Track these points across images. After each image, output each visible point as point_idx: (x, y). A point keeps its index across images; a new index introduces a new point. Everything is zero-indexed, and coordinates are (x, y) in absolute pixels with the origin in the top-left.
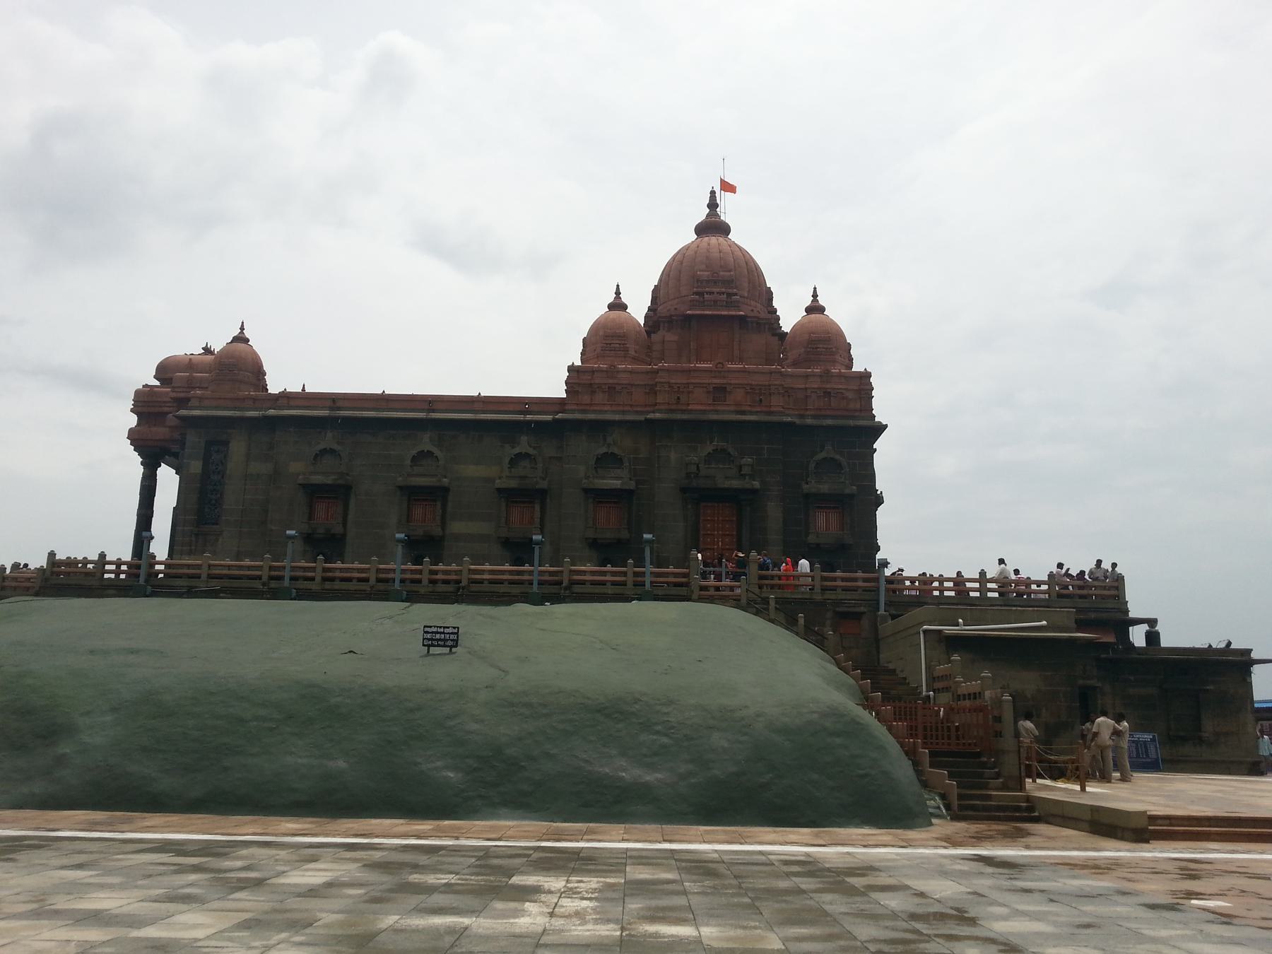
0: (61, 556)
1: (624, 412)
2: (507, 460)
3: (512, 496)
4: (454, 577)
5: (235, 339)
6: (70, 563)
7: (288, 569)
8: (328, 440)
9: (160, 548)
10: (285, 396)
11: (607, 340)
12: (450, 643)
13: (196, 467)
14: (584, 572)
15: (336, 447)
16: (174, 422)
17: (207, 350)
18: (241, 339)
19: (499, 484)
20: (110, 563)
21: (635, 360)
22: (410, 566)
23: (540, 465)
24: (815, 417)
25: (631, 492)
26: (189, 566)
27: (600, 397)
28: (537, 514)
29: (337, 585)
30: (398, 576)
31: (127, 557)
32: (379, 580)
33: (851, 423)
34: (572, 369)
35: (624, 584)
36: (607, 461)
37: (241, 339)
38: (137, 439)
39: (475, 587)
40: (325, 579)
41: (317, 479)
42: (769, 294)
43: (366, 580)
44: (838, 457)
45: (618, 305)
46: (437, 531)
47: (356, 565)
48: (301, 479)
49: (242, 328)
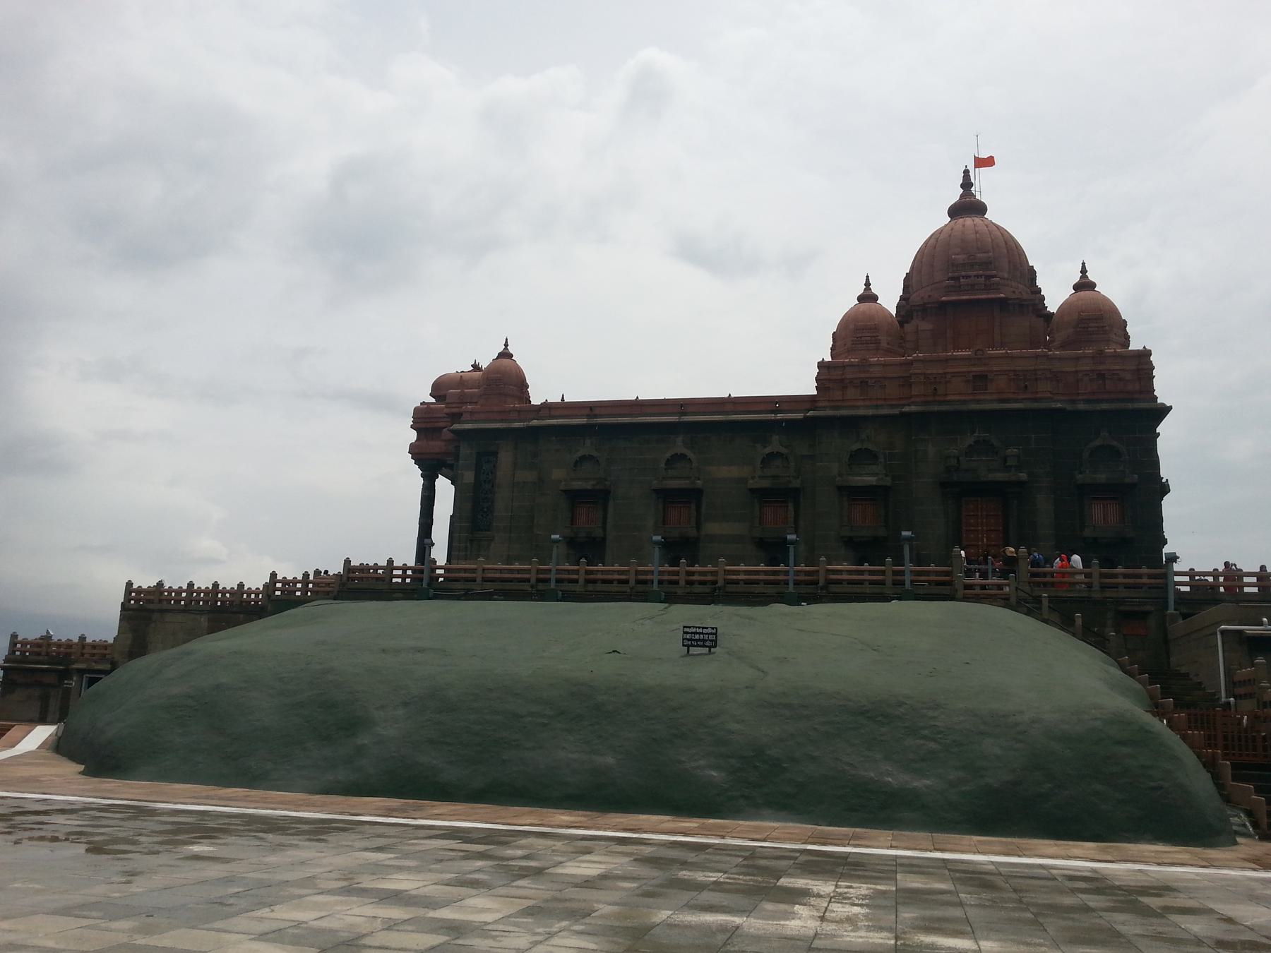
0: (355, 563)
1: (877, 407)
3: (763, 496)
4: (709, 578)
5: (501, 355)
6: (363, 568)
7: (554, 572)
8: (587, 447)
9: (440, 554)
10: (547, 407)
11: (859, 333)
12: (708, 643)
13: (469, 477)
14: (840, 572)
15: (594, 453)
16: (451, 436)
17: (476, 367)
18: (505, 355)
19: (752, 484)
20: (398, 568)
21: (888, 352)
22: (667, 568)
24: (1088, 401)
25: (886, 489)
26: (465, 570)
27: (851, 393)
28: (791, 514)
29: (600, 587)
30: (656, 578)
31: (411, 562)
32: (638, 582)
33: (1130, 406)
34: (821, 365)
35: (882, 583)
36: (860, 458)
37: (505, 355)
38: (417, 453)
39: (731, 588)
40: (588, 581)
41: (577, 485)
42: (1032, 273)
43: (626, 582)
44: (1114, 443)
45: (868, 297)
46: (692, 533)
47: (617, 567)
49: (506, 345)
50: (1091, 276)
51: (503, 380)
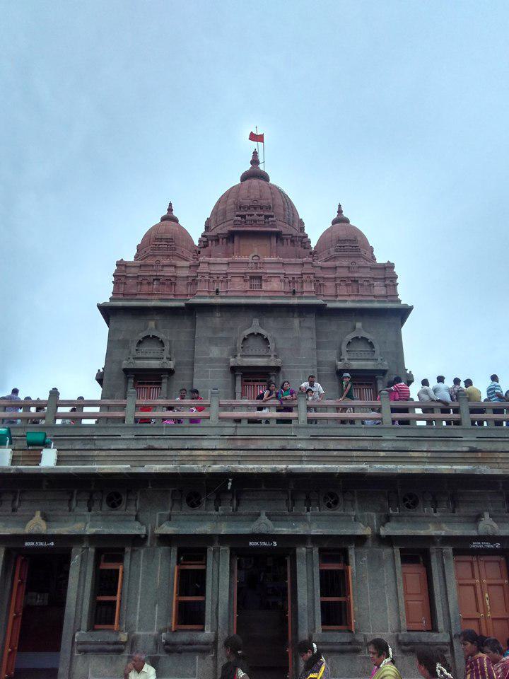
25: (170, 372)
34: (121, 264)
50: (345, 214)
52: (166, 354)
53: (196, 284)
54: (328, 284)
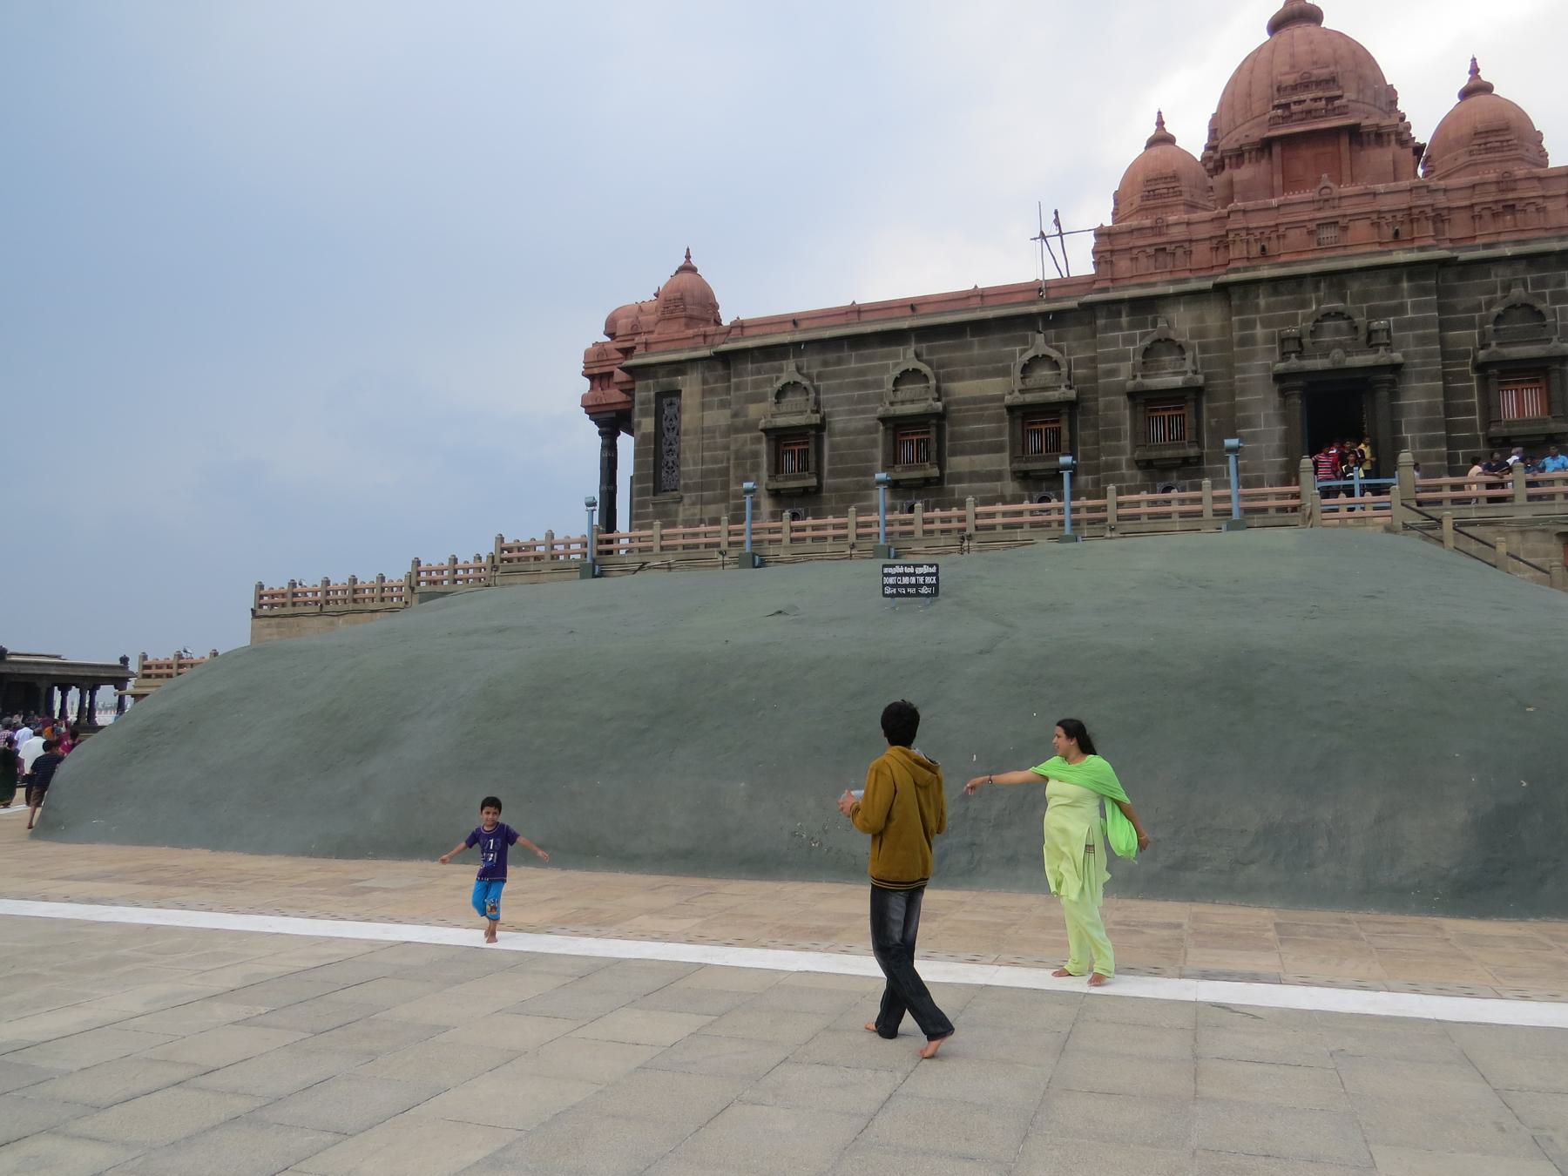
0: (509, 541)
2: (1019, 368)
4: (955, 524)
5: (682, 269)
8: (788, 371)
10: (740, 326)
12: (924, 590)
18: (687, 268)
19: (1008, 399)
23: (1064, 370)
25: (1199, 391)
34: (1101, 233)
37: (687, 268)
41: (781, 421)
45: (1162, 139)
48: (762, 424)
49: (688, 257)
50: (1485, 76)
51: (688, 302)
52: (1188, 365)
53: (1227, 247)
54: (1455, 216)
